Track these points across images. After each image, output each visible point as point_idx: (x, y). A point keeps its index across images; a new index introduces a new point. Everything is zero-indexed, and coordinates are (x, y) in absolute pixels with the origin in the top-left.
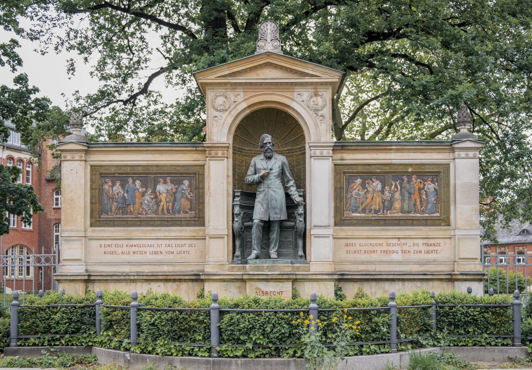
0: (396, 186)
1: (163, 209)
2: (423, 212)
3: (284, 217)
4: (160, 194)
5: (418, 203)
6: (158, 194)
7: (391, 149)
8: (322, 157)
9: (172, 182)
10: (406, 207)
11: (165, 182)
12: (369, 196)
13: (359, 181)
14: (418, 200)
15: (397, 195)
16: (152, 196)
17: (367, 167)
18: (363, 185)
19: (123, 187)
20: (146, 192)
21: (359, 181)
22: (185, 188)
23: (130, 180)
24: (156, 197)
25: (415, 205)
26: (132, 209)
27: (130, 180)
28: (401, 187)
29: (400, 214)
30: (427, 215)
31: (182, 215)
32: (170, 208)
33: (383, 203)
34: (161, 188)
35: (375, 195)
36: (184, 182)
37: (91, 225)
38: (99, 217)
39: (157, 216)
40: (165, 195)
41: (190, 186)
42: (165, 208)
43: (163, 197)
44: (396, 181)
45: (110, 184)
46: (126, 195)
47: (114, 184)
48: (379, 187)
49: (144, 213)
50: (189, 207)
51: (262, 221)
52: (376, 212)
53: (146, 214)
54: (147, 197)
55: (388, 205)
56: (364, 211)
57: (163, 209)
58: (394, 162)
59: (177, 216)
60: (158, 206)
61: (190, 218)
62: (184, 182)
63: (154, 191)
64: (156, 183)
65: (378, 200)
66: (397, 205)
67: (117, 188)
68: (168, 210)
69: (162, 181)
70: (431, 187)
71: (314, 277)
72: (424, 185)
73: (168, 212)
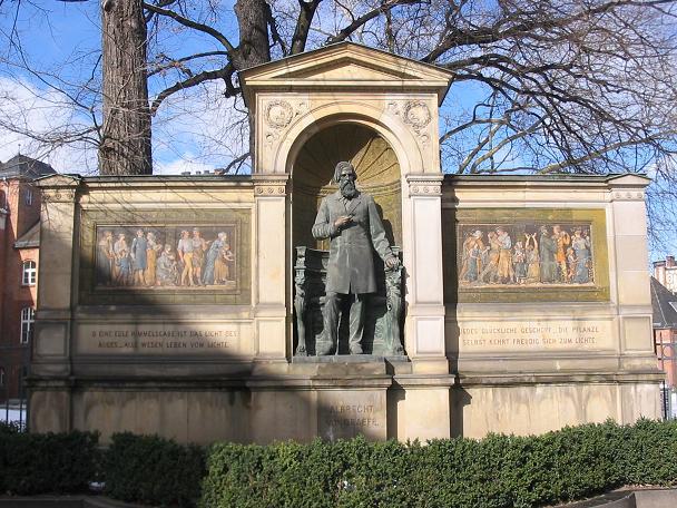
0: (531, 241)
1: (187, 277)
2: (571, 280)
3: (371, 289)
4: (183, 253)
5: (564, 267)
6: (180, 254)
7: (525, 187)
8: (426, 195)
9: (202, 235)
10: (546, 272)
11: (191, 236)
12: (493, 256)
13: (478, 234)
14: (564, 263)
15: (533, 256)
16: (172, 257)
17: (490, 212)
18: (485, 240)
19: (129, 242)
20: (163, 250)
21: (478, 234)
22: (220, 244)
23: (140, 233)
24: (177, 258)
25: (559, 269)
26: (141, 278)
27: (140, 233)
28: (538, 242)
29: (539, 285)
30: (577, 285)
31: (216, 287)
32: (198, 275)
33: (514, 268)
34: (184, 244)
35: (502, 255)
36: (220, 235)
37: (81, 302)
38: (93, 291)
39: (179, 288)
40: (191, 255)
41: (230, 240)
42: (190, 275)
43: (187, 258)
44: (531, 233)
45: (110, 238)
46: (132, 255)
47: (116, 238)
48: (508, 242)
49: (159, 283)
50: (226, 273)
51: (339, 295)
52: (506, 280)
53: (162, 285)
54: (162, 259)
55: (521, 268)
56: (486, 280)
57: (187, 277)
58: (528, 205)
59: (209, 287)
60: (180, 271)
61: (228, 291)
62: (220, 235)
63: (174, 250)
64: (177, 237)
65: (506, 264)
66: (534, 270)
67: (121, 244)
68: (194, 277)
69: (187, 234)
70: (579, 242)
71: (419, 382)
72: (571, 240)
73: (196, 282)
